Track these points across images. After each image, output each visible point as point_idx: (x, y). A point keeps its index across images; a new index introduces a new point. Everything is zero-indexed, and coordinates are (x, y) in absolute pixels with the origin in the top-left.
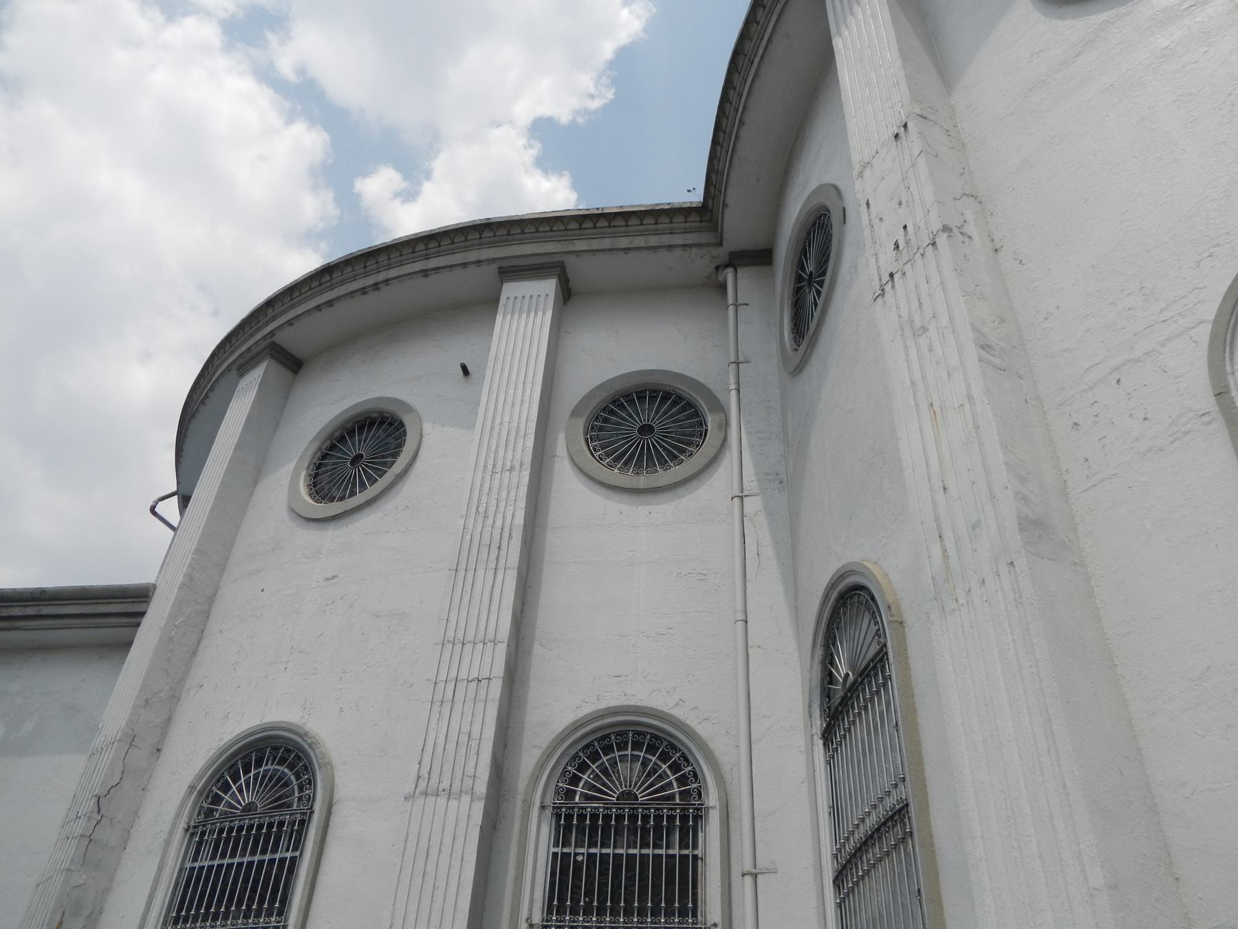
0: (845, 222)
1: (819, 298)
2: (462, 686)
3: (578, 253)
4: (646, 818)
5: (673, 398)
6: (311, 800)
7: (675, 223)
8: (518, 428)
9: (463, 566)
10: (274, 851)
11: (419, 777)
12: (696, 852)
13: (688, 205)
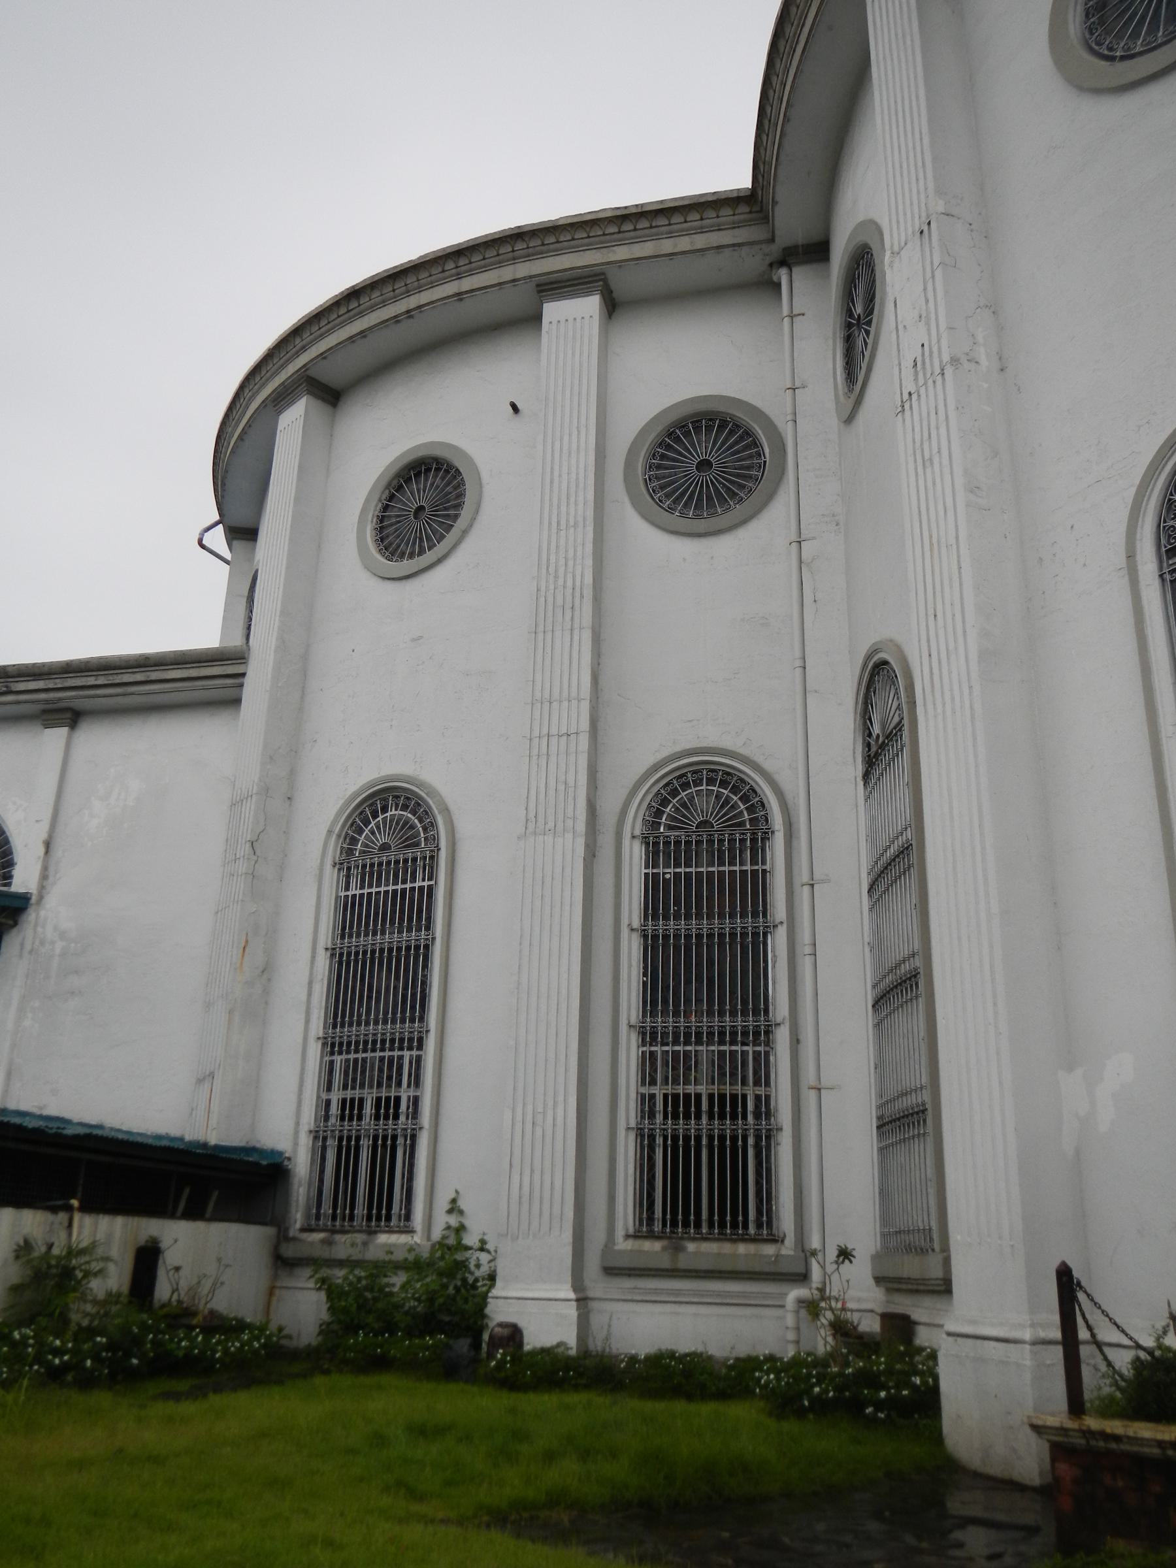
1: (868, 338)
2: (554, 741)
3: (620, 264)
4: (721, 841)
6: (435, 839)
7: (722, 216)
8: (577, 479)
9: (541, 628)
10: (414, 880)
11: (527, 820)
12: (764, 867)
13: (735, 195)
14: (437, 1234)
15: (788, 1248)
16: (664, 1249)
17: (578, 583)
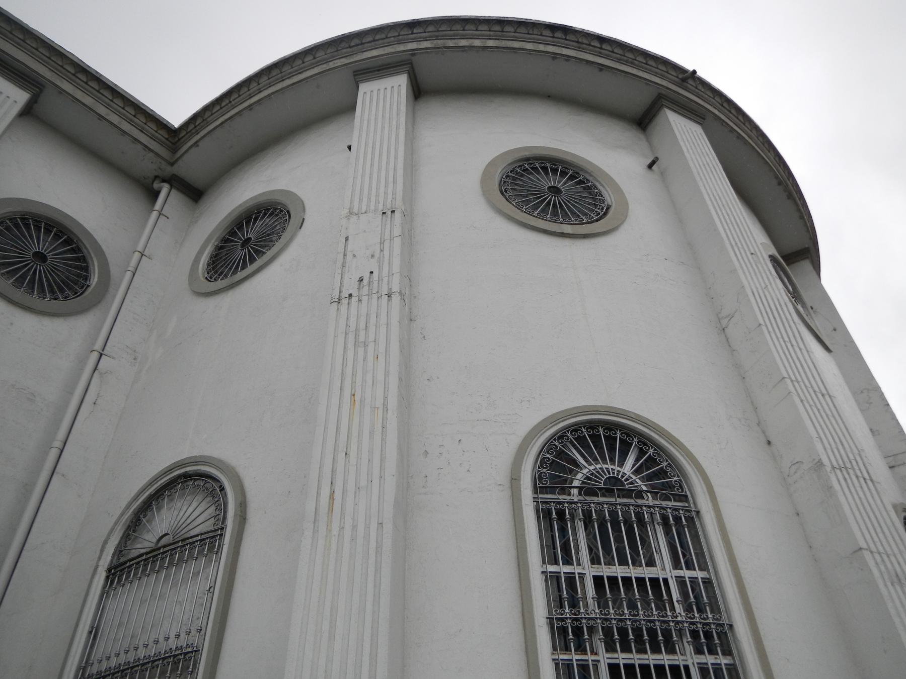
0: (300, 228)
3: (62, 91)
5: (74, 245)
13: (165, 122)
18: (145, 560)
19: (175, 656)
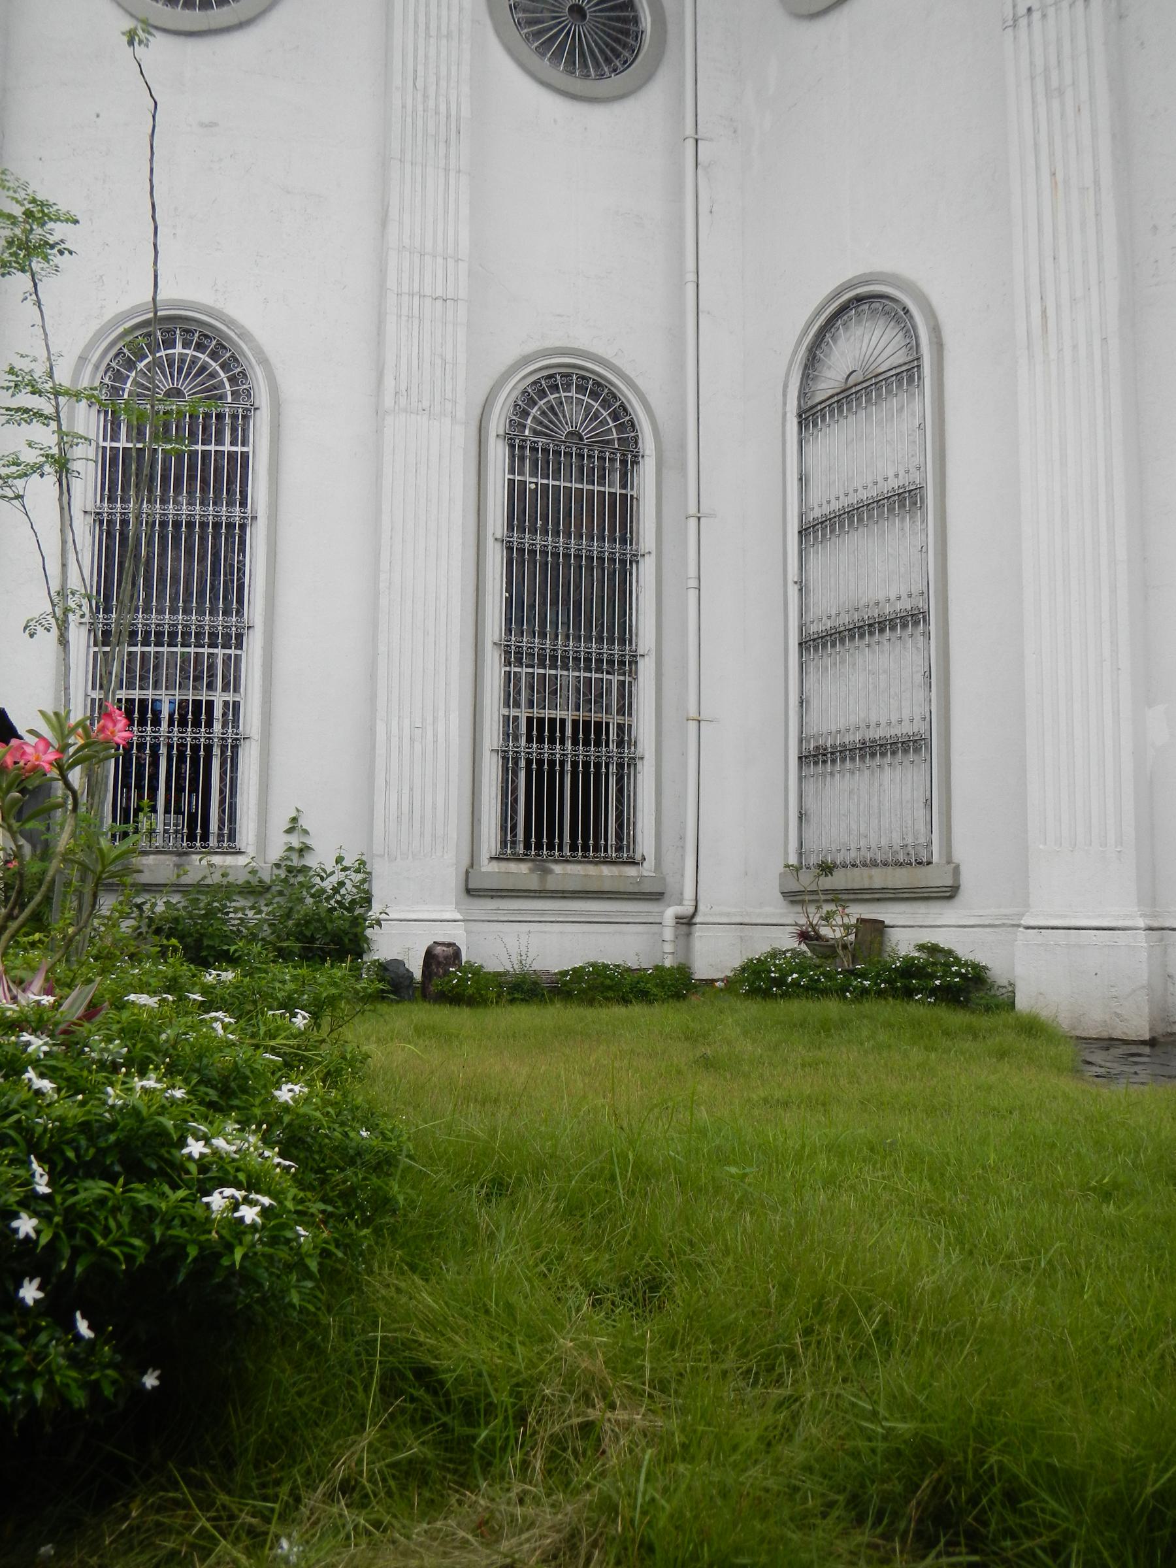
14: (276, 852)
15: (648, 868)
16: (532, 870)
17: (453, 112)
18: (838, 401)
19: (899, 494)
